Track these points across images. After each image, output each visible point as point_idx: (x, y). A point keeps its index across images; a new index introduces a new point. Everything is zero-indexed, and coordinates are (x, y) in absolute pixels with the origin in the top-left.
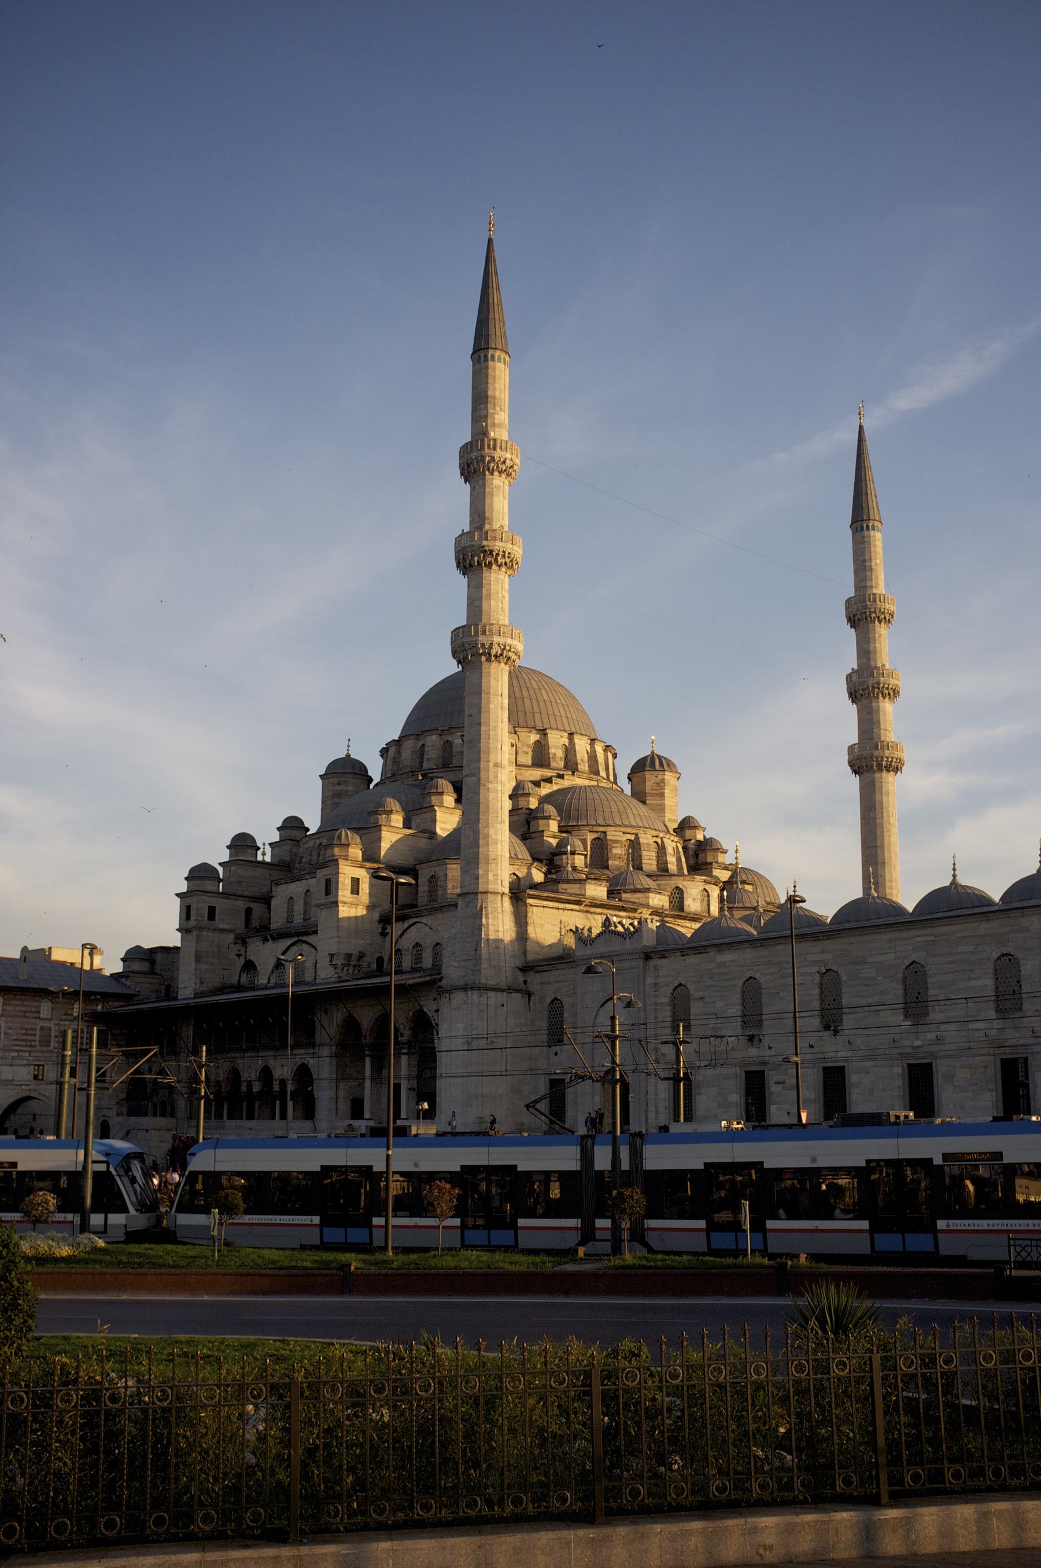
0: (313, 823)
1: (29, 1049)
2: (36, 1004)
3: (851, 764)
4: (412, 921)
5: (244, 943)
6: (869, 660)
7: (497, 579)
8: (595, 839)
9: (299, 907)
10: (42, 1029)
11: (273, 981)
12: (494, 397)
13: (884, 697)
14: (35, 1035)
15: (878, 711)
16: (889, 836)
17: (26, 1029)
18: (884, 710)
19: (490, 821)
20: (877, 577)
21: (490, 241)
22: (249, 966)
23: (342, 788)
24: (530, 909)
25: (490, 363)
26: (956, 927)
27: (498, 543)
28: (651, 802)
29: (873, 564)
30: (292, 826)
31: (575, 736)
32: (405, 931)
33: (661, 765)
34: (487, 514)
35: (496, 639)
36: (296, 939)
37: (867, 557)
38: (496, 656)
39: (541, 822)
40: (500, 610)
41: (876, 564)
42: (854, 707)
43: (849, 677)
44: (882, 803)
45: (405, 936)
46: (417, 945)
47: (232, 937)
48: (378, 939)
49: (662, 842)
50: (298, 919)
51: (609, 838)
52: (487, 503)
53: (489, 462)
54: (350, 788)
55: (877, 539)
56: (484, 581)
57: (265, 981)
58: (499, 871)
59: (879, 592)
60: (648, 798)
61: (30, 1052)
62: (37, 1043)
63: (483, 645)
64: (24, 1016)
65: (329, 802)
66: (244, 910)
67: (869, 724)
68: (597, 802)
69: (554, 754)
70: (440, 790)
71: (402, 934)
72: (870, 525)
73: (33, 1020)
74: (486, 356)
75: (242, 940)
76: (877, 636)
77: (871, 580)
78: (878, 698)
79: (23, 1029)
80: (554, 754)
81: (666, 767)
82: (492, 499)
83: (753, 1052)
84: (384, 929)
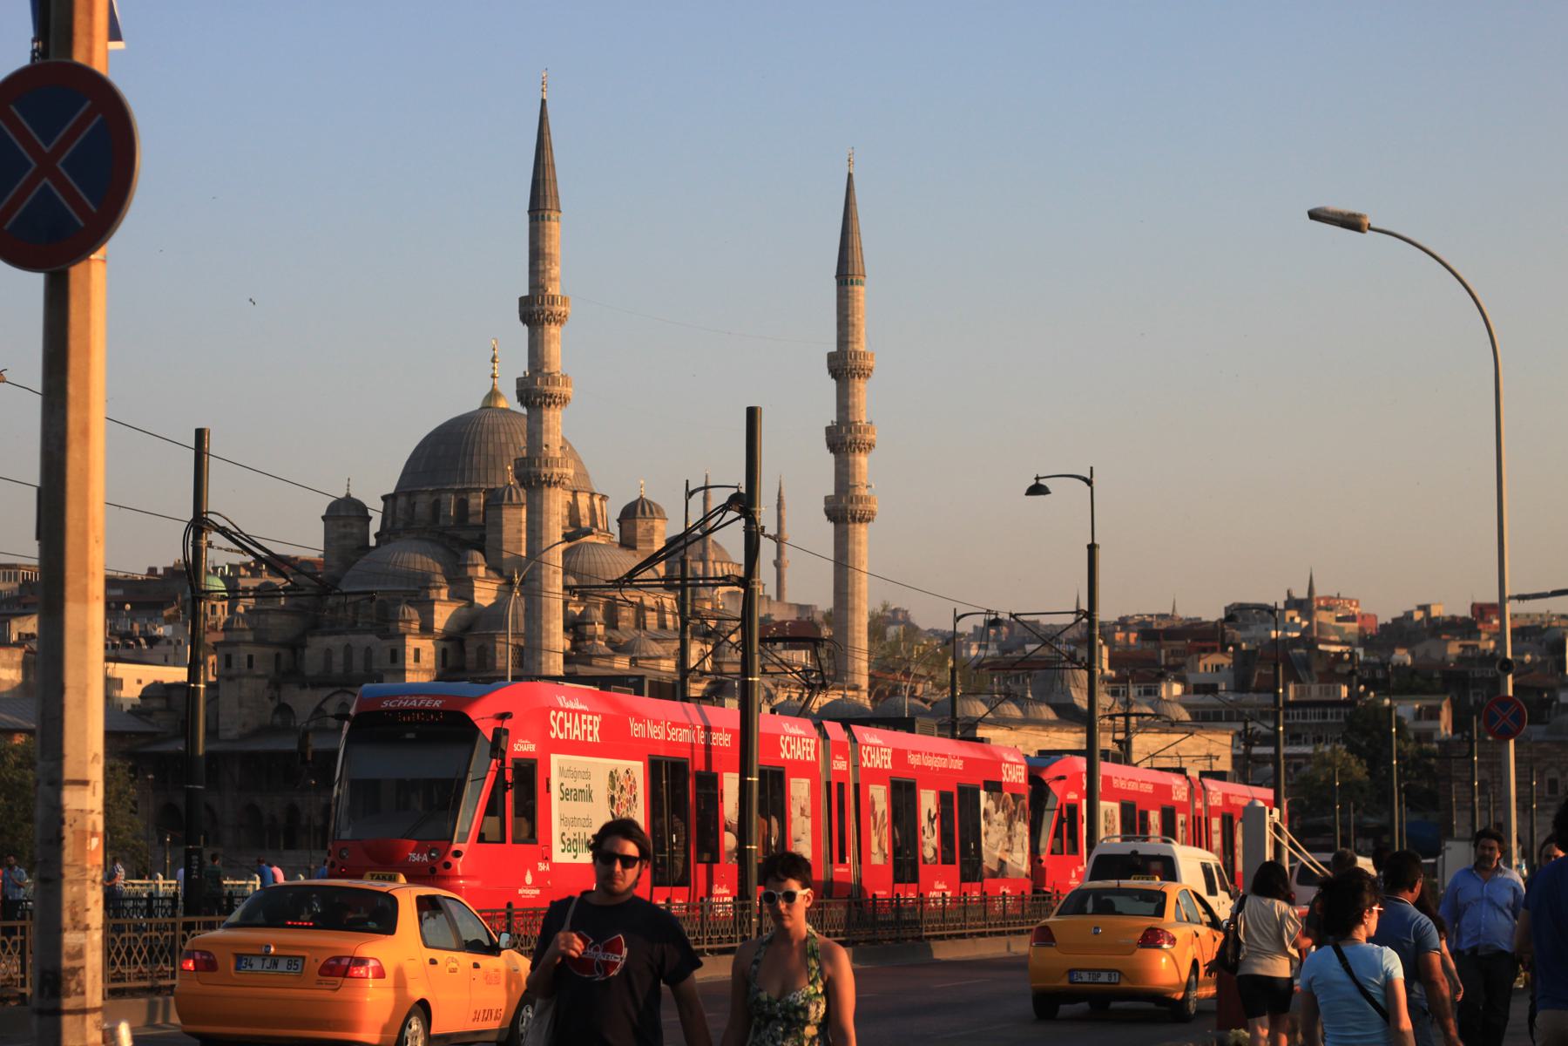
3: (827, 512)
6: (848, 414)
7: (554, 416)
9: (338, 658)
11: (312, 724)
12: (550, 254)
13: (860, 451)
15: (854, 465)
16: (860, 583)
19: (551, 618)
20: (858, 333)
21: (543, 102)
22: (284, 709)
23: (348, 530)
25: (547, 223)
27: (557, 388)
29: (855, 319)
31: (578, 494)
33: (651, 512)
34: (546, 360)
35: (556, 470)
36: (339, 689)
37: (850, 312)
38: (555, 483)
41: (858, 319)
43: (828, 430)
44: (854, 553)
47: (266, 681)
49: (662, 602)
50: (338, 669)
52: (546, 350)
53: (548, 316)
54: (355, 530)
56: (544, 418)
59: (863, 350)
60: (638, 544)
63: (545, 475)
68: (606, 565)
70: (475, 562)
72: (855, 279)
74: (543, 216)
77: (853, 335)
78: (854, 451)
81: (656, 515)
82: (549, 346)
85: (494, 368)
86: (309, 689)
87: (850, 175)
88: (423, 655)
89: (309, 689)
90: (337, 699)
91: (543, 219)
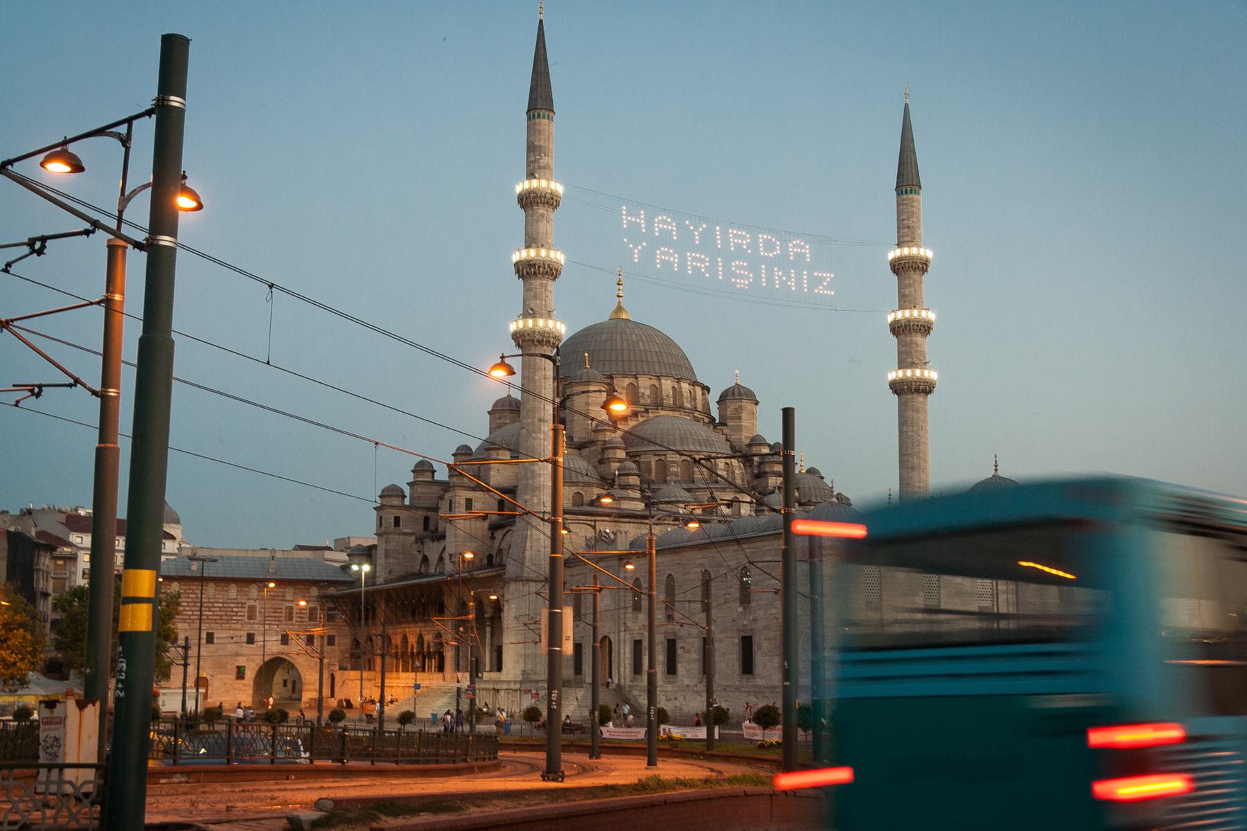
1: (277, 623)
2: (282, 590)
4: (507, 529)
5: (422, 543)
8: (659, 460)
14: (281, 613)
17: (275, 609)
21: (541, 21)
22: (425, 559)
26: (763, 543)
28: (730, 424)
39: (610, 451)
40: (543, 306)
42: (895, 340)
45: (505, 540)
47: (413, 538)
48: (488, 542)
51: (668, 459)
54: (508, 421)
57: (433, 571)
58: (542, 496)
61: (278, 625)
62: (283, 619)
64: (274, 599)
66: (423, 518)
69: (643, 393)
71: (503, 538)
73: (280, 602)
79: (272, 608)
80: (643, 393)
83: (670, 628)
84: (493, 534)
86: (436, 542)
87: (906, 106)
88: (477, 506)
89: (436, 542)
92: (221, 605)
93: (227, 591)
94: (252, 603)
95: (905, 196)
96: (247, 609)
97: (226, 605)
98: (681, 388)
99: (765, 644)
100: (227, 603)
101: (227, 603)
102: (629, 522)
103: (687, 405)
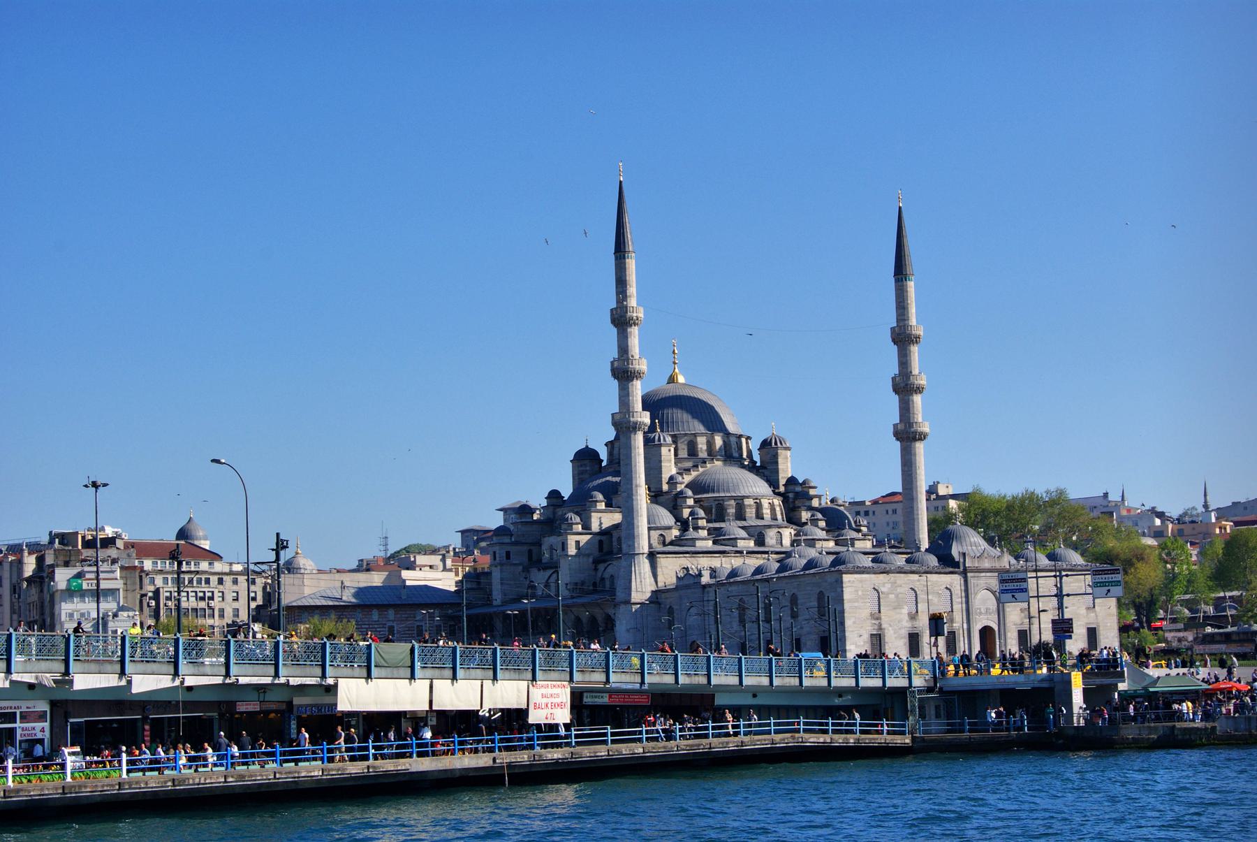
0: (567, 492)
2: (413, 612)
4: (608, 563)
5: (528, 571)
10: (418, 626)
18: (913, 401)
24: (658, 559)
30: (554, 495)
32: (606, 568)
43: (893, 379)
46: (612, 576)
47: (521, 568)
54: (588, 468)
55: (911, 286)
62: (416, 635)
65: (576, 478)
67: (906, 410)
69: (701, 448)
71: (605, 570)
75: (526, 570)
76: (908, 352)
80: (701, 448)
84: (596, 566)
85: (674, 357)
86: (542, 571)
89: (542, 571)
90: (555, 575)
91: (624, 258)
92: (367, 626)
93: (371, 615)
94: (390, 624)
95: (900, 284)
96: (387, 629)
97: (371, 626)
98: (730, 441)
99: (809, 643)
100: (372, 625)
101: (372, 625)
102: (703, 557)
103: (736, 455)
